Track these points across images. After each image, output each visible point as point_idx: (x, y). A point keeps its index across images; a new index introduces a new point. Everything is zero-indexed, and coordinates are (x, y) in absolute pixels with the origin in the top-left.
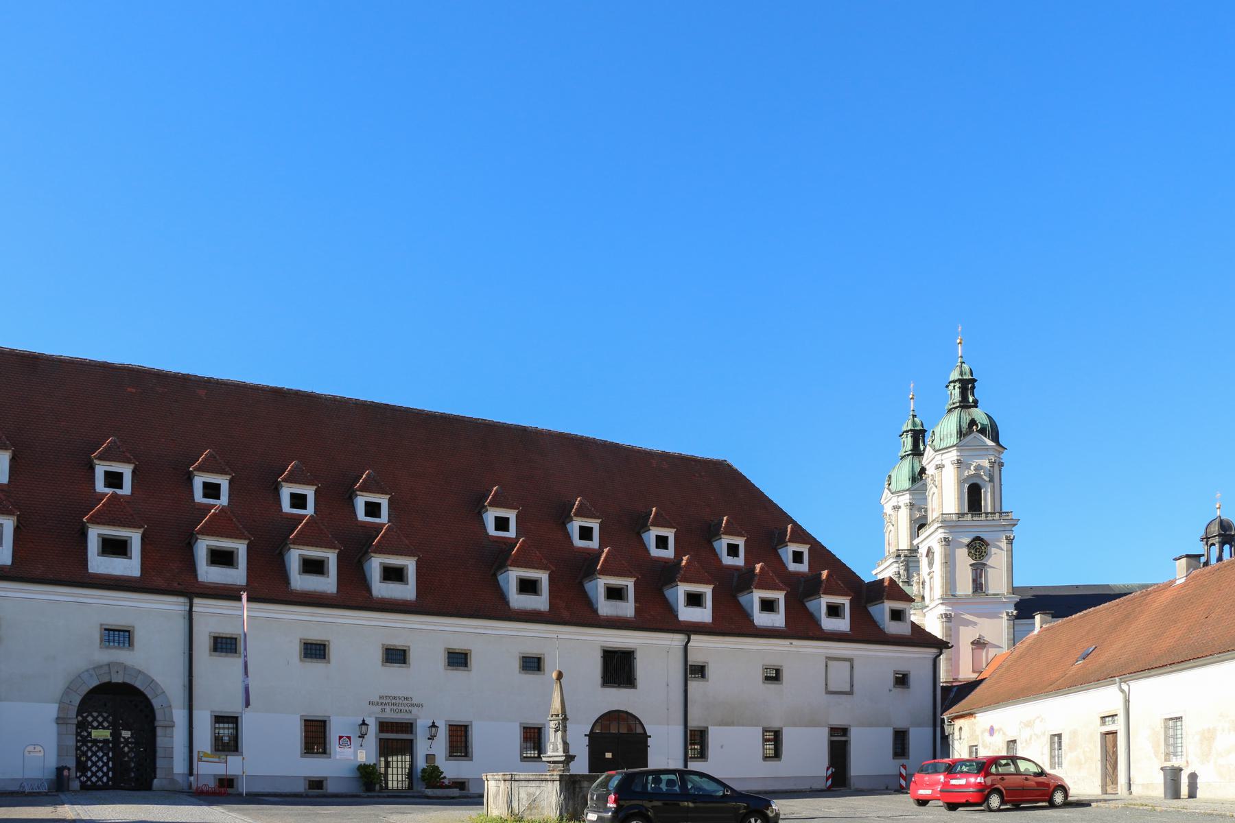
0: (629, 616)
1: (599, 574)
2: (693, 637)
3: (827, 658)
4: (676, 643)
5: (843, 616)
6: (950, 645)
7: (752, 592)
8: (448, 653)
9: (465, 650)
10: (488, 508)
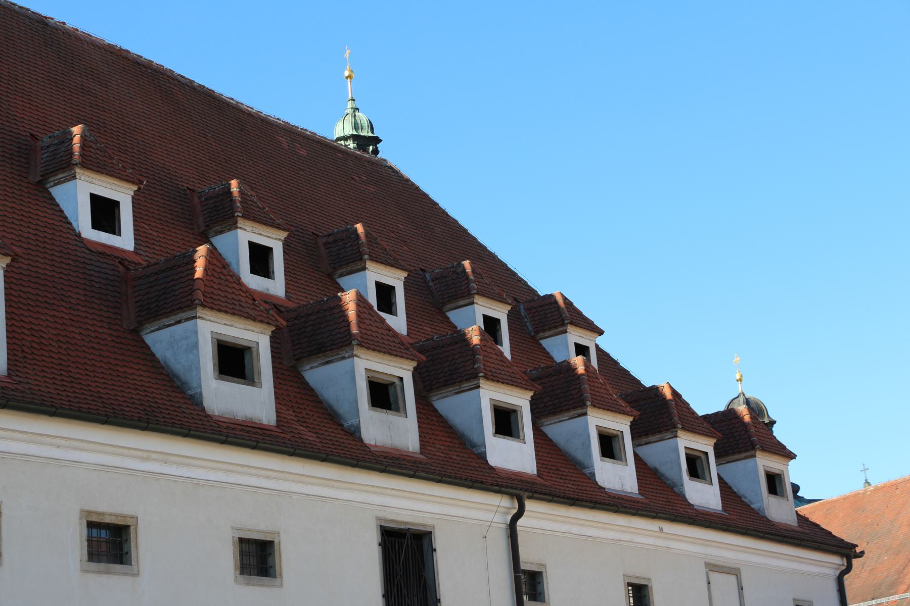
0: (411, 450)
1: (360, 345)
2: (530, 506)
3: (707, 565)
4: (488, 516)
5: (708, 479)
6: (858, 550)
7: (585, 414)
8: (91, 525)
9: (125, 517)
10: (78, 171)
